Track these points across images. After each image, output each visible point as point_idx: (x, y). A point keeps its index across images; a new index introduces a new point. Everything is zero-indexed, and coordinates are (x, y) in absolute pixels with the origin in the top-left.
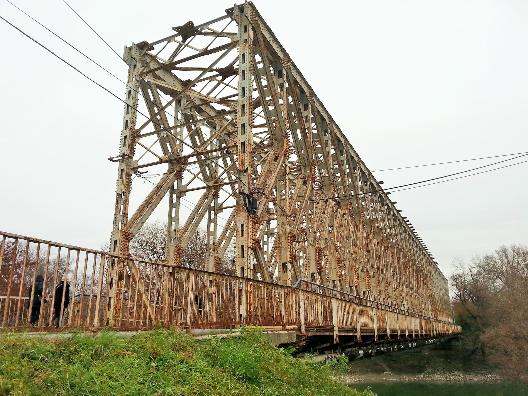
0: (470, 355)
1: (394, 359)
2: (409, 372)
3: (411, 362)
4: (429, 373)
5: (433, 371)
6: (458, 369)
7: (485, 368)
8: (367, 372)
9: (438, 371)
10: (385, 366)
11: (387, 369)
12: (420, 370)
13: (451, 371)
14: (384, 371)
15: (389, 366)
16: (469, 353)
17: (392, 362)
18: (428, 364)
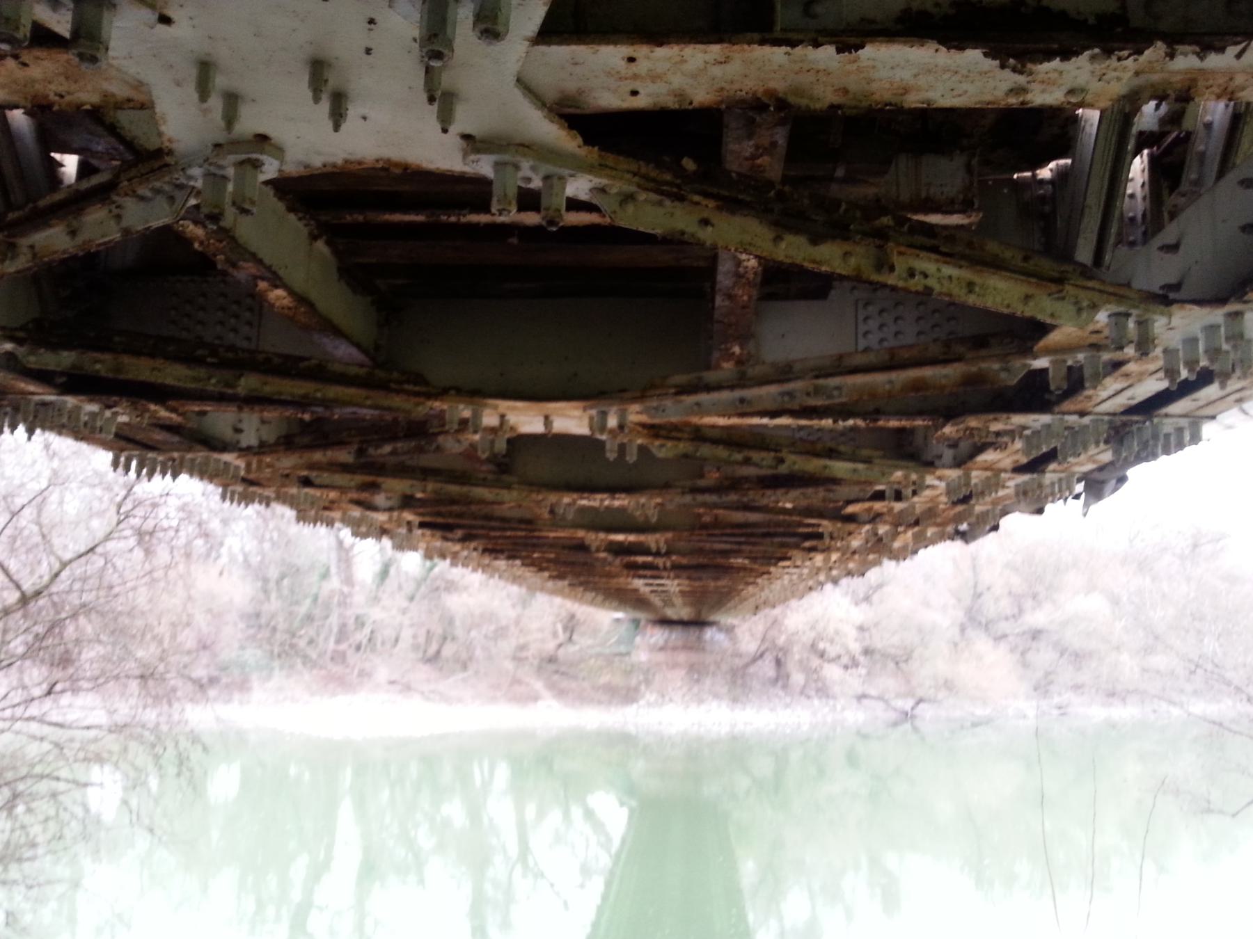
0: (747, 666)
1: (563, 669)
2: (600, 702)
3: (604, 679)
4: (649, 704)
5: (660, 700)
6: (716, 696)
7: (777, 695)
8: (493, 699)
9: (671, 700)
10: (539, 685)
11: (545, 693)
12: (629, 696)
13: (701, 701)
14: (535, 698)
15: (551, 686)
16: (746, 660)
17: (556, 677)
18: (648, 682)
